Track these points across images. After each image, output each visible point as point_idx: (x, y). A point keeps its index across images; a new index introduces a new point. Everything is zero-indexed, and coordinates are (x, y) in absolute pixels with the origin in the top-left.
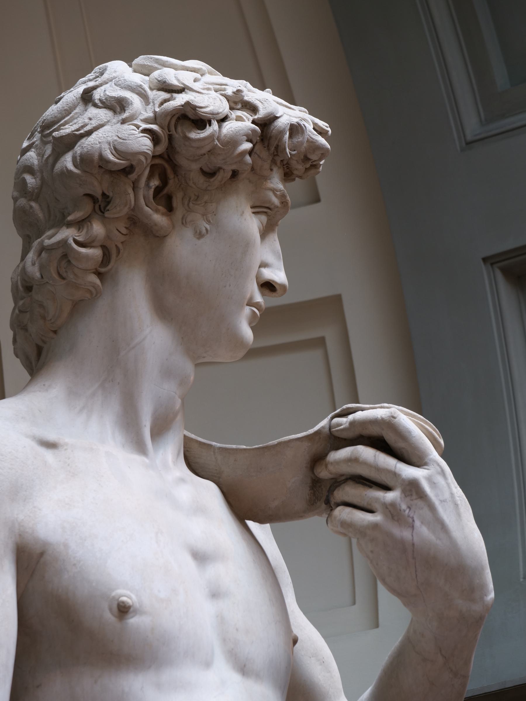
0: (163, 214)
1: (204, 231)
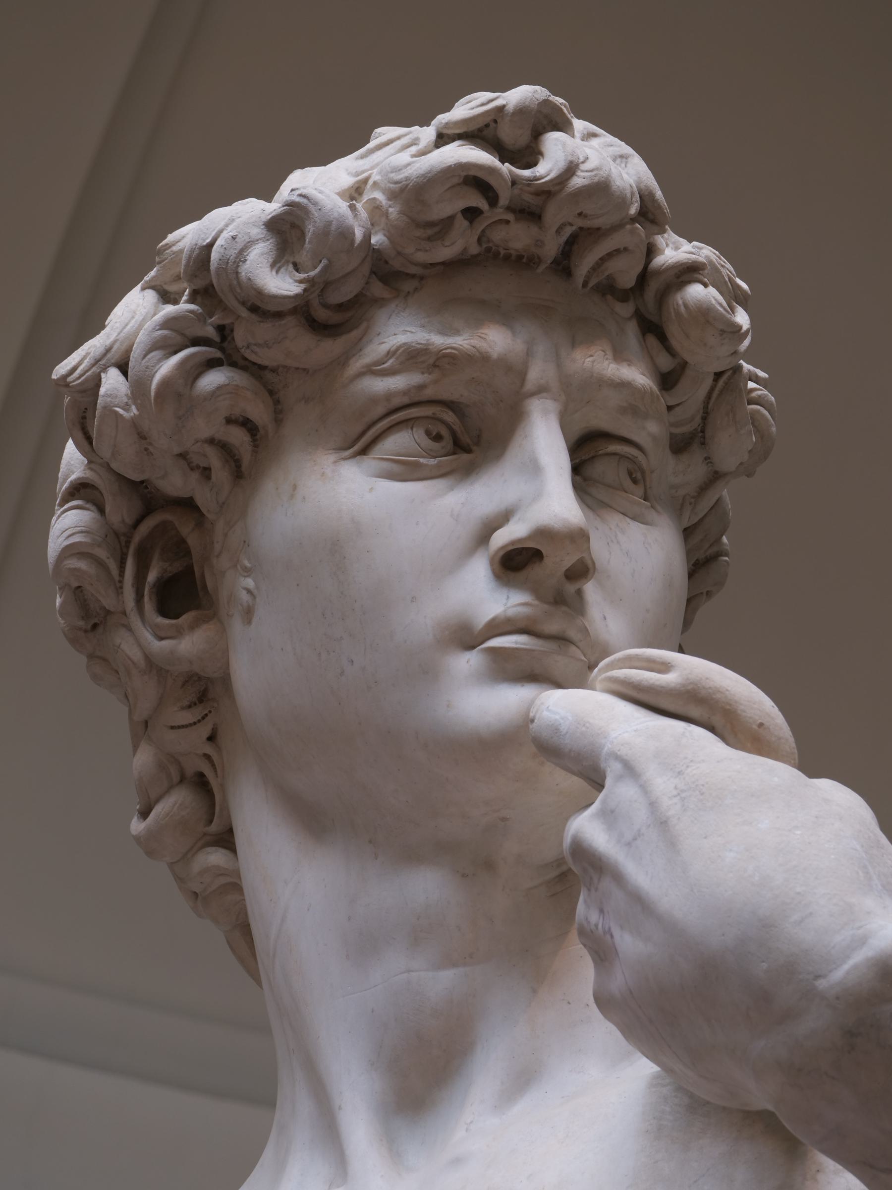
0: (193, 627)
1: (244, 597)
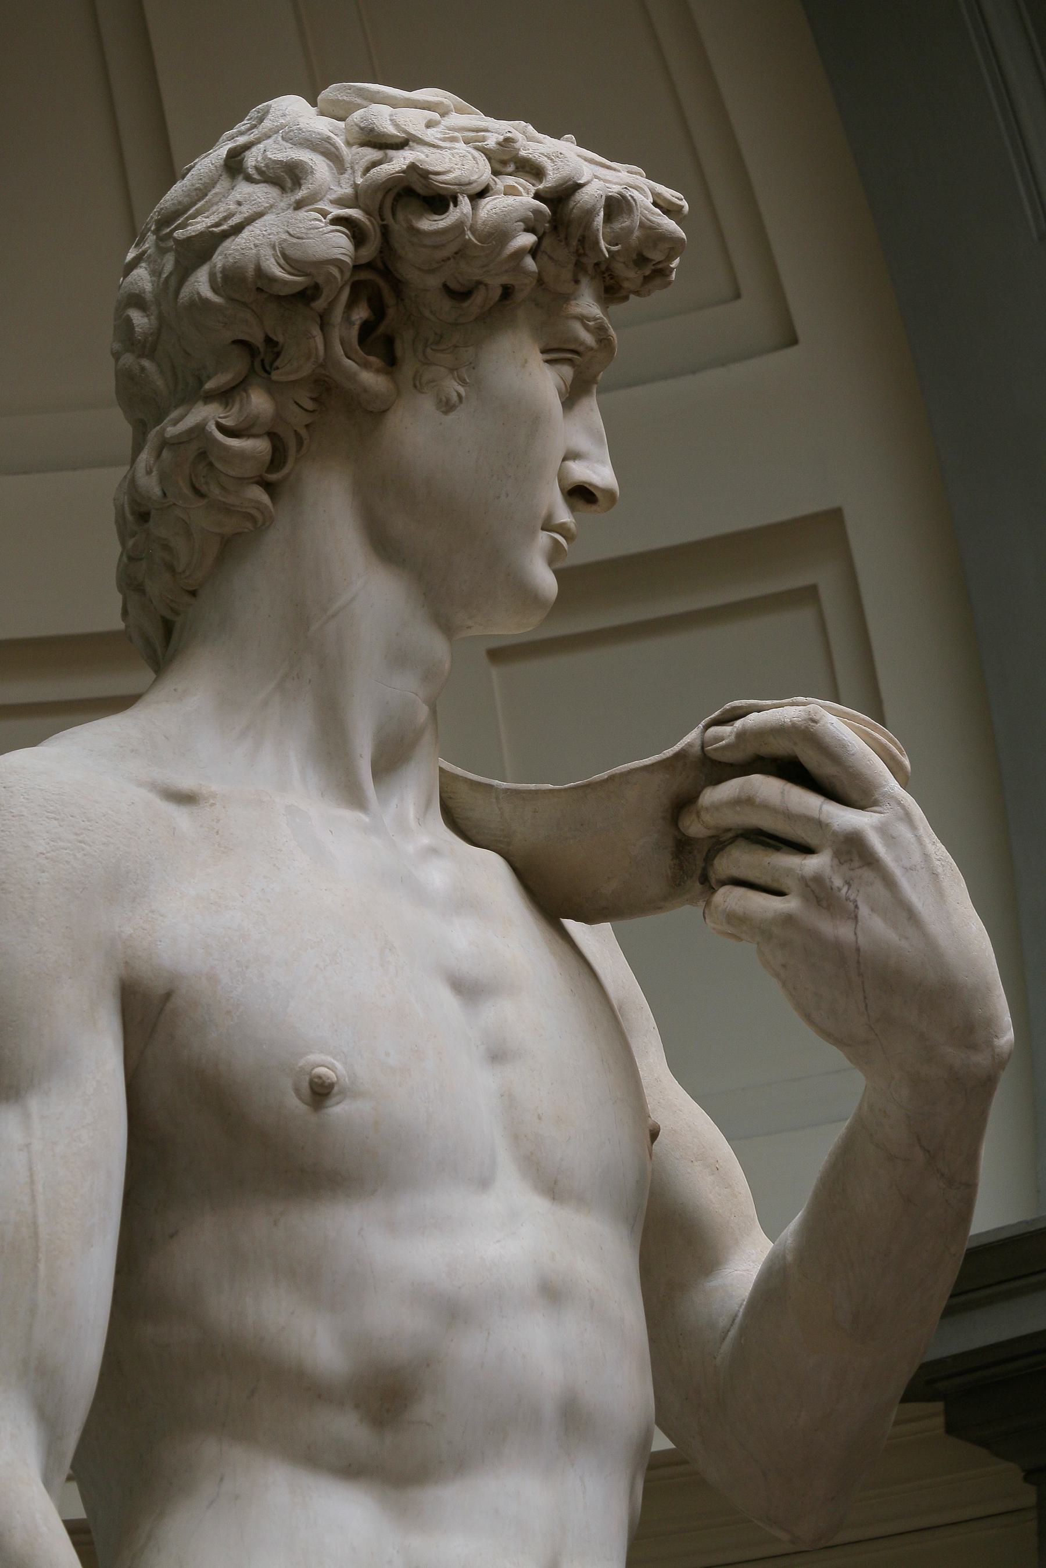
0: (378, 371)
1: (455, 398)
